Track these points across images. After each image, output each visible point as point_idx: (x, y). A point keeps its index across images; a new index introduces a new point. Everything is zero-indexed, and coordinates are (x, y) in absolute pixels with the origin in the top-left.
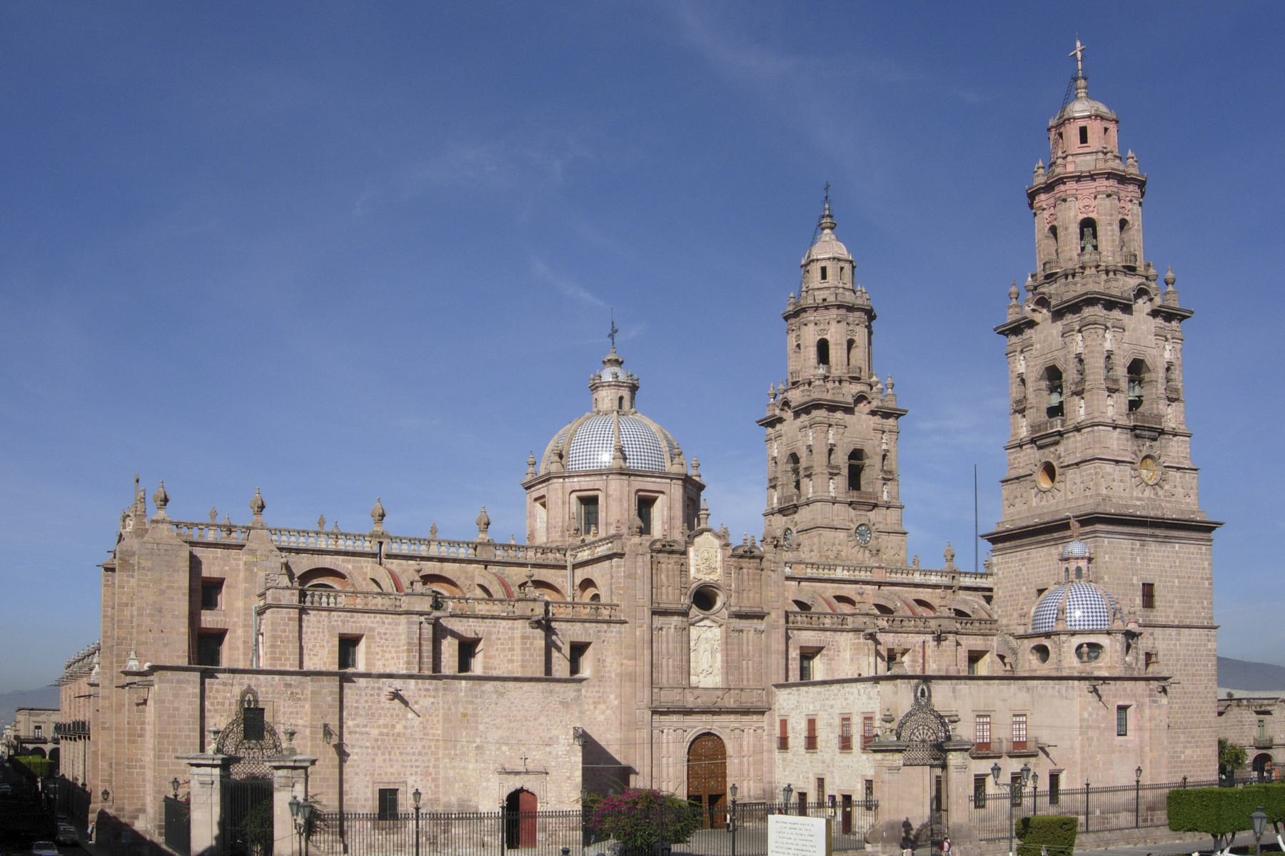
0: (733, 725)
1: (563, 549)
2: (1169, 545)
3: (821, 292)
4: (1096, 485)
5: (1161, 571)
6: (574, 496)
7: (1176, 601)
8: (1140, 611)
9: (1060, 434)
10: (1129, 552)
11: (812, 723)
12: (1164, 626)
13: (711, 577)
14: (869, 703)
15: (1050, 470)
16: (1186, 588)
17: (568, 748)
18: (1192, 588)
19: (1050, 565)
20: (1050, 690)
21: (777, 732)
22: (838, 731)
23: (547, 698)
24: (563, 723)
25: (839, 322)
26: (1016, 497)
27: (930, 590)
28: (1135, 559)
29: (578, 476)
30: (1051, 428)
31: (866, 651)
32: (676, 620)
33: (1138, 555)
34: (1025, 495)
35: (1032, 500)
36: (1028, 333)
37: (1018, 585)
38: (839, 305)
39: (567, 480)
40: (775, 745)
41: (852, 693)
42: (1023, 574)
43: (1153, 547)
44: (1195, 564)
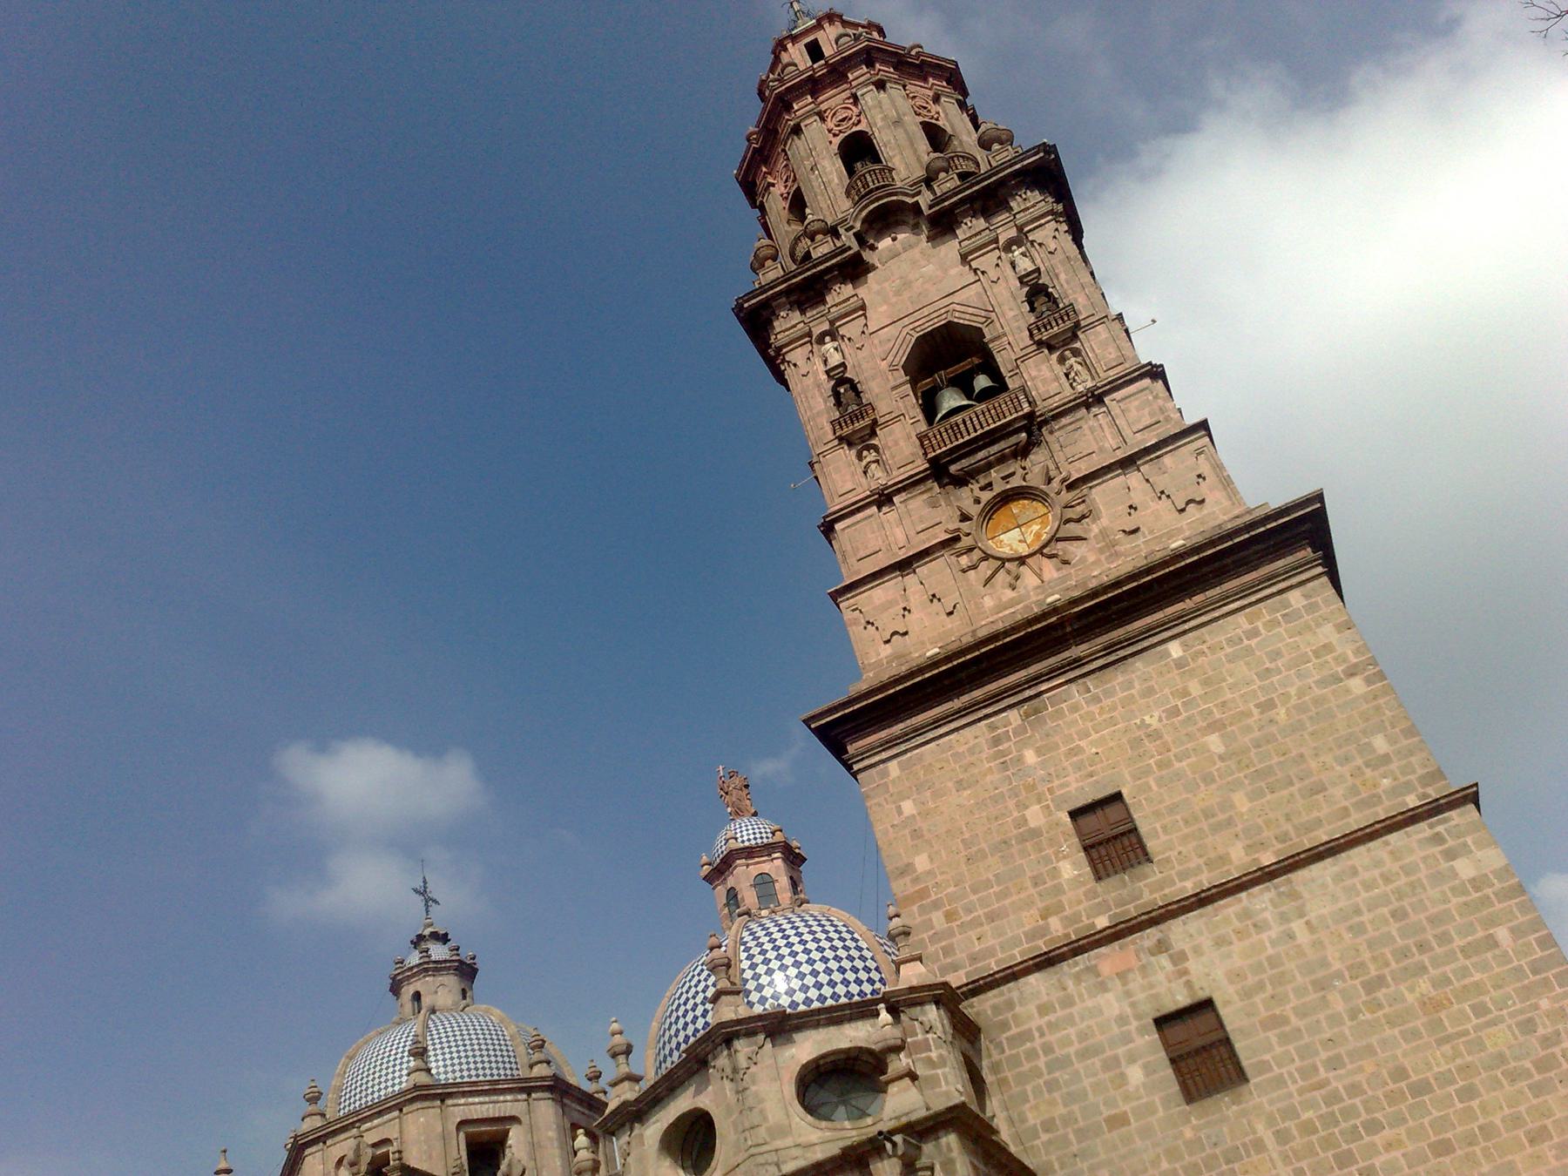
8: (1091, 895)
10: (987, 752)
12: (1202, 900)
28: (1020, 759)
33: (1022, 745)
44: (1277, 654)
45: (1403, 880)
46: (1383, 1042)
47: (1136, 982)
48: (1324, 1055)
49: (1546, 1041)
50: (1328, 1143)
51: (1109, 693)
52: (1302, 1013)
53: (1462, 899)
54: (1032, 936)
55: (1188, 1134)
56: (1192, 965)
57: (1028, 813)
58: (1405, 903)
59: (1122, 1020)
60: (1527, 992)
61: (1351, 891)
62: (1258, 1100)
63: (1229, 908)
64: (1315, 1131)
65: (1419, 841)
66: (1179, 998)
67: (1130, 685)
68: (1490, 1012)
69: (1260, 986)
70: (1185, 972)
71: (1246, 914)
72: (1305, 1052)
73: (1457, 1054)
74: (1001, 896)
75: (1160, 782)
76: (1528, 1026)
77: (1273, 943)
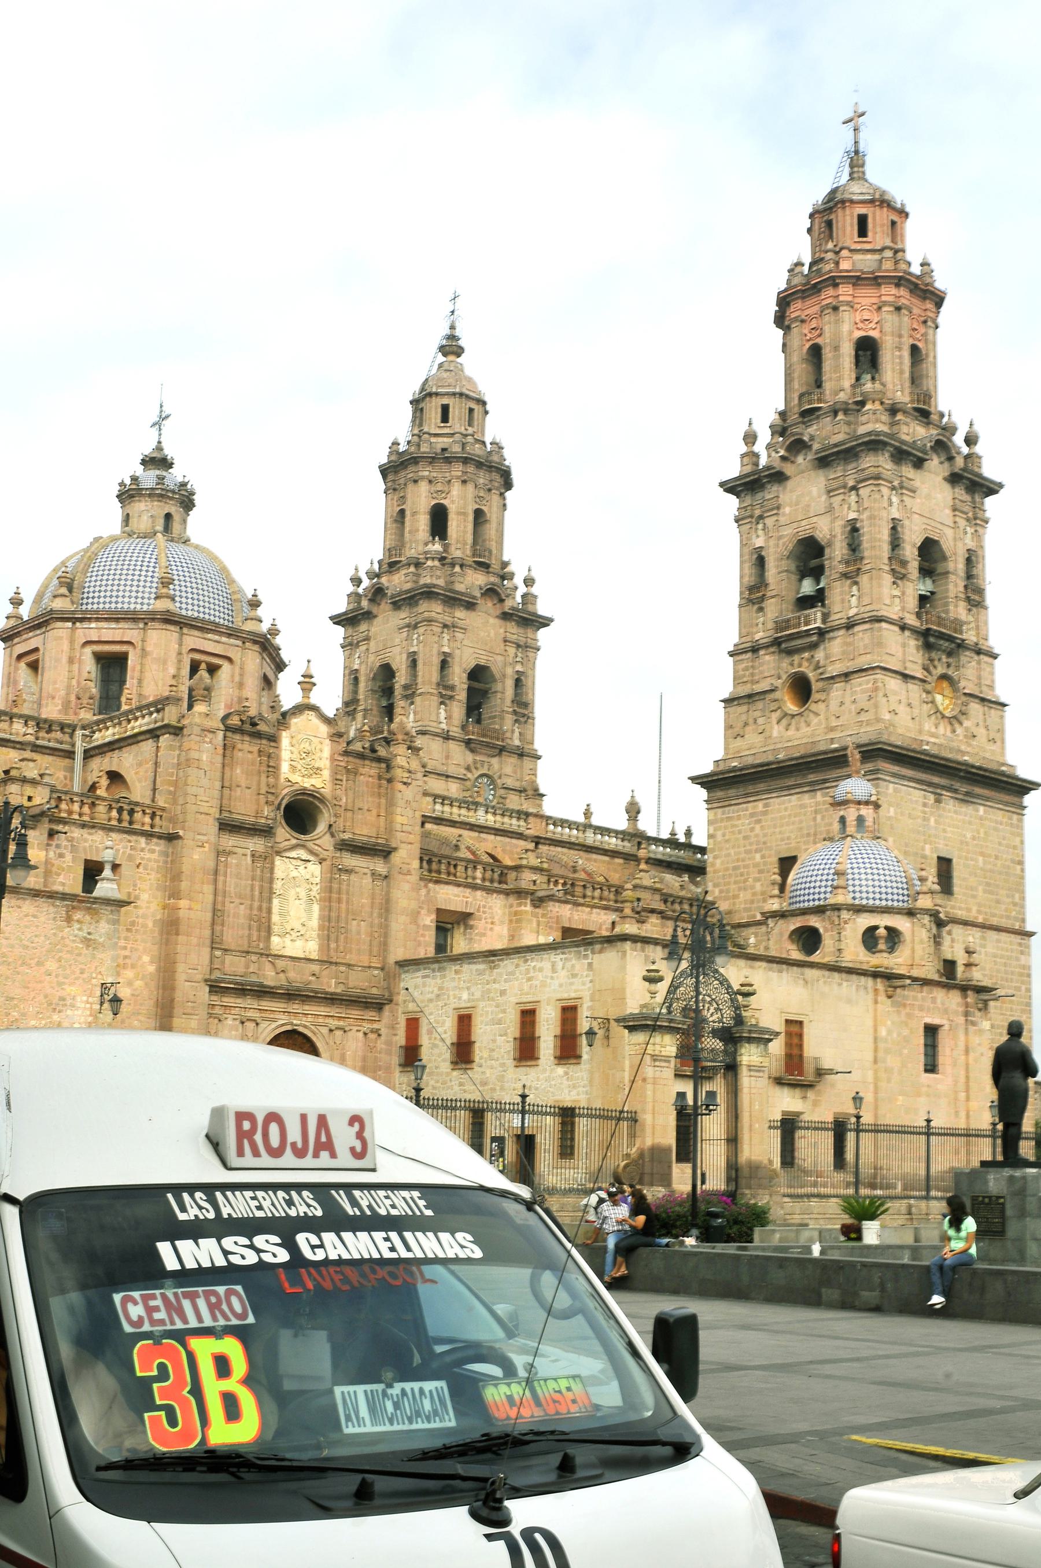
0: (333, 1023)
1: (69, 726)
2: (971, 807)
3: (440, 440)
4: (876, 706)
5: (962, 842)
6: (88, 650)
7: (980, 888)
9: (821, 633)
10: (921, 808)
11: (464, 1022)
13: (313, 781)
14: (572, 984)
15: (802, 689)
16: (991, 871)
17: (90, 1019)
18: (1000, 873)
19: (801, 822)
20: (835, 987)
21: (401, 1039)
22: (513, 1030)
23: (60, 929)
24: (85, 976)
25: (464, 482)
26: (746, 724)
27: (606, 858)
28: (929, 820)
29: (98, 619)
30: (806, 624)
31: (535, 925)
32: (256, 844)
33: (932, 814)
34: (760, 721)
35: (772, 728)
36: (772, 491)
37: (747, 852)
38: (466, 458)
39: (78, 624)
40: (395, 1059)
41: (541, 970)
42: (757, 836)
43: (950, 805)
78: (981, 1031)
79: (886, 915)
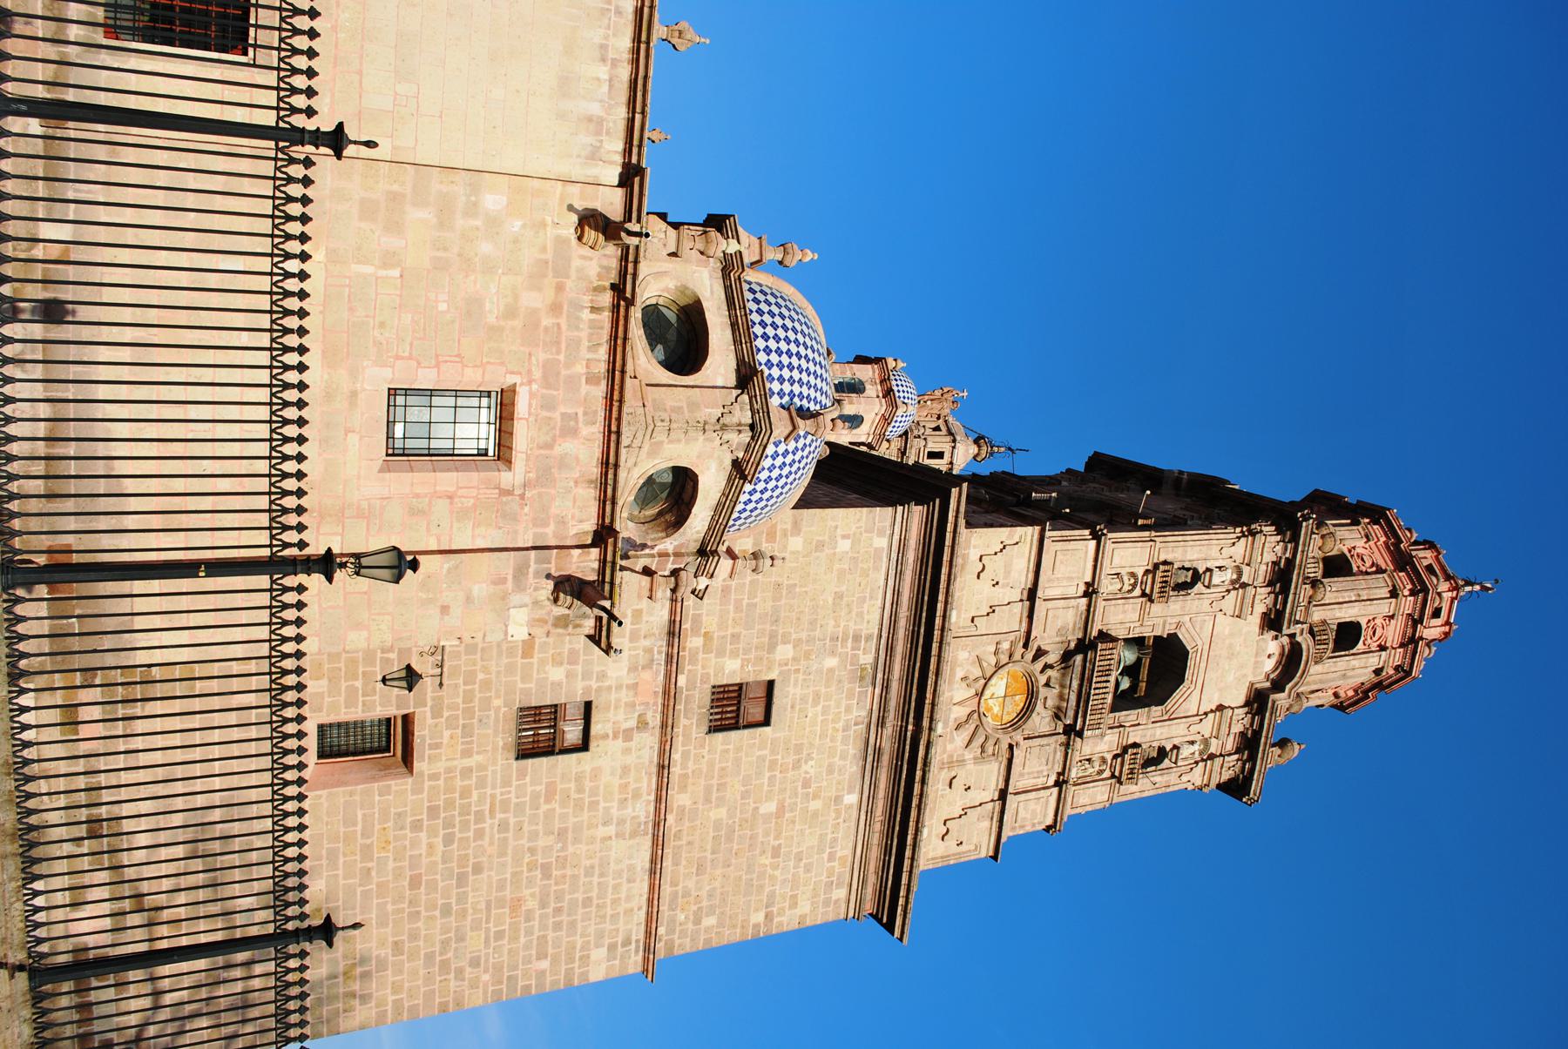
5: (798, 749)
7: (722, 813)
10: (852, 627)
12: (663, 768)
18: (750, 870)
28: (833, 653)
44: (808, 870)
45: (609, 912)
46: (504, 865)
47: (626, 697)
48: (512, 821)
49: (460, 972)
50: (450, 804)
51: (845, 740)
52: (549, 815)
53: (578, 947)
54: (697, 620)
55: (497, 702)
56: (620, 743)
57: (790, 647)
58: (594, 909)
59: (602, 676)
60: (498, 968)
61: (619, 874)
62: (500, 763)
63: (648, 784)
64: (461, 798)
65: (631, 930)
66: (599, 726)
67: (843, 758)
68: (495, 942)
69: (580, 790)
70: (615, 737)
71: (637, 795)
72: (520, 808)
73: (475, 911)
74: (738, 602)
75: (762, 759)
76: (475, 963)
77: (607, 809)
78: (501, 604)
79: (729, 332)
